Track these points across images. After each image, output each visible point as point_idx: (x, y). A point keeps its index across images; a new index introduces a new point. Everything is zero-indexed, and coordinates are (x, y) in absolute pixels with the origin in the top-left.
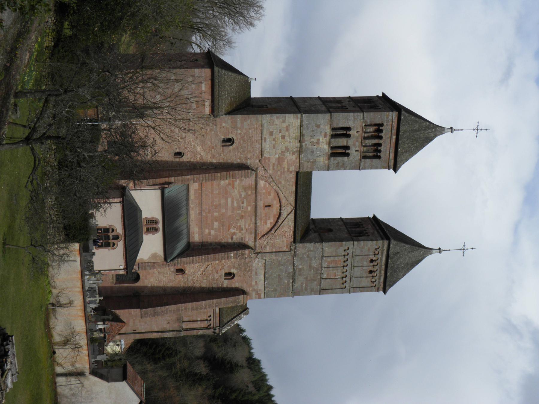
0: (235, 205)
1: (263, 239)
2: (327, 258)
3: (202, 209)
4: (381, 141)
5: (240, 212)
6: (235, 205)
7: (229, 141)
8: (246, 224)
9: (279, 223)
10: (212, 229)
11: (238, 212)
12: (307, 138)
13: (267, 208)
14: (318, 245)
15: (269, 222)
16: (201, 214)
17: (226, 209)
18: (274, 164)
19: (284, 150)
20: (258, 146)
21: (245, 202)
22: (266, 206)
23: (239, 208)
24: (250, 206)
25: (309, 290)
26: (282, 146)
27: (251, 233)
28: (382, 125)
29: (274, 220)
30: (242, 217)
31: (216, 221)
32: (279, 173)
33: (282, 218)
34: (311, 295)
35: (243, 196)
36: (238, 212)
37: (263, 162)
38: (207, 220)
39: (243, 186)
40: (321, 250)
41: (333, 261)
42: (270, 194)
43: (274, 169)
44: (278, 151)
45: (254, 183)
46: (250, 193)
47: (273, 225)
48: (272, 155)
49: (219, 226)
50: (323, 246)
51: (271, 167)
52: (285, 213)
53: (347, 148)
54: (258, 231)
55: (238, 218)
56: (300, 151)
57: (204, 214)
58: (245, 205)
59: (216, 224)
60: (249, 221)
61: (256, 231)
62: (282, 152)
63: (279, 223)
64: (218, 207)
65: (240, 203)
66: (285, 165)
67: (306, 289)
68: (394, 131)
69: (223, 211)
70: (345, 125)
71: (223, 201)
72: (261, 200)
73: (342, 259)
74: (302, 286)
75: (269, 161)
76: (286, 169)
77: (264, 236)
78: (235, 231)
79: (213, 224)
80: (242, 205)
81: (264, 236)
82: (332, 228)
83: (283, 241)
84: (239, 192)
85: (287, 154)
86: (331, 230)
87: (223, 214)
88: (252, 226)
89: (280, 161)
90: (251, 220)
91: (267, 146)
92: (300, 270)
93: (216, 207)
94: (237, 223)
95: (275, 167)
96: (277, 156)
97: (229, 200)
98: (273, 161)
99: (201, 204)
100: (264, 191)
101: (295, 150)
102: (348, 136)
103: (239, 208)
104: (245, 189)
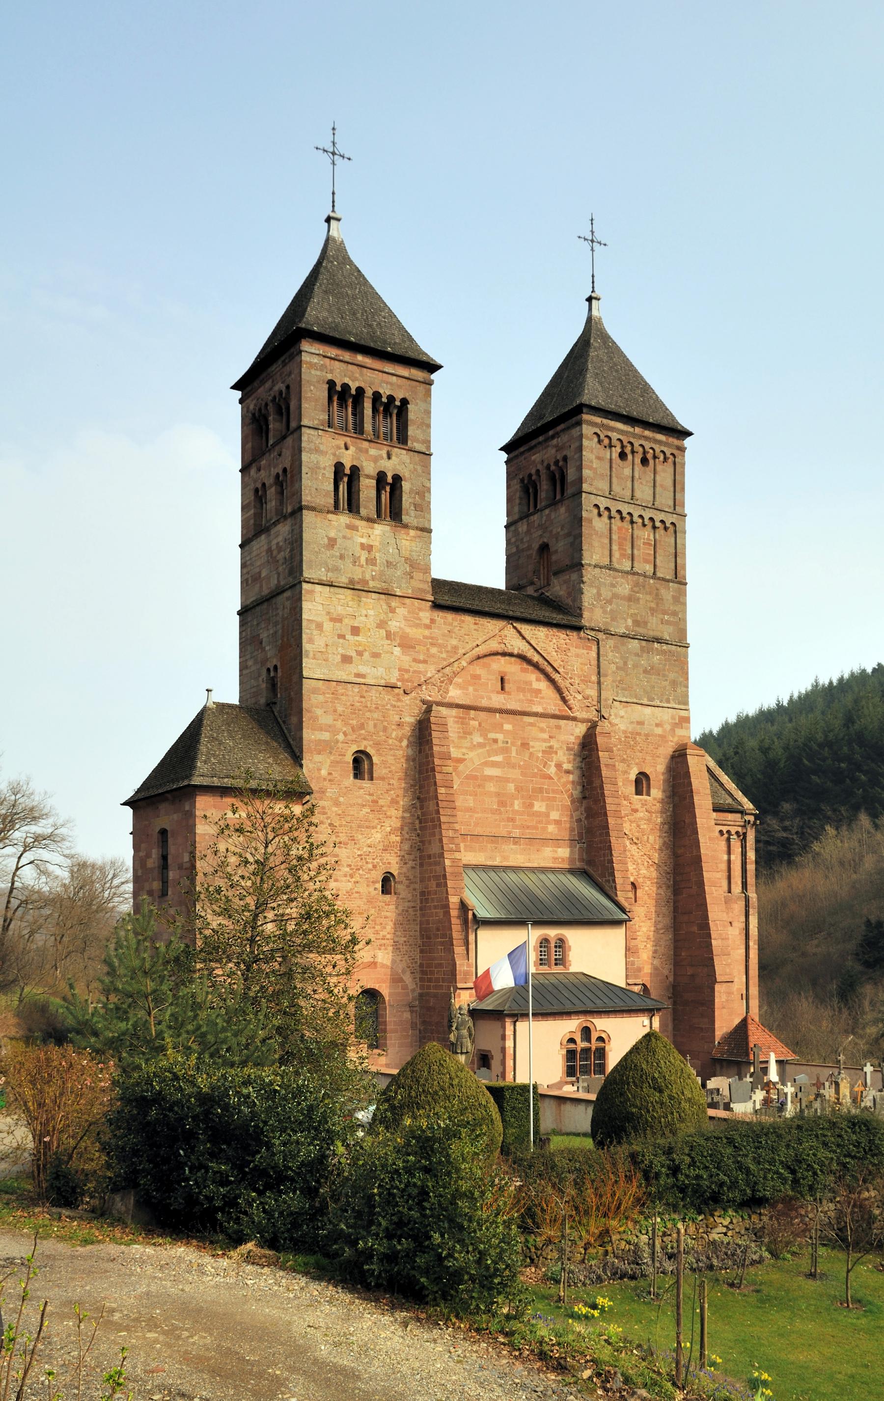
0: (499, 758)
2: (614, 559)
3: (507, 838)
5: (514, 748)
6: (499, 758)
9: (541, 661)
10: (547, 815)
11: (514, 754)
13: (507, 686)
14: (588, 574)
15: (536, 685)
16: (516, 840)
17: (507, 780)
18: (415, 660)
19: (383, 633)
20: (373, 693)
21: (492, 735)
22: (503, 689)
24: (502, 726)
26: (374, 638)
27: (558, 727)
29: (532, 672)
30: (525, 745)
31: (531, 805)
32: (434, 650)
33: (530, 654)
36: (514, 754)
38: (528, 827)
39: (460, 737)
40: (597, 570)
41: (620, 544)
42: (476, 677)
47: (542, 676)
48: (391, 664)
49: (543, 800)
50: (590, 565)
51: (421, 667)
52: (517, 645)
55: (527, 755)
57: (516, 833)
58: (500, 737)
59: (539, 806)
60: (534, 732)
61: (554, 717)
63: (541, 661)
65: (495, 746)
66: (416, 633)
69: (511, 787)
71: (491, 787)
72: (490, 699)
73: (617, 523)
75: (407, 671)
76: (427, 632)
77: (564, 700)
78: (553, 764)
79: (538, 814)
80: (500, 744)
81: (564, 700)
82: (536, 546)
83: (577, 656)
84: (473, 747)
85: (394, 625)
86: (544, 548)
87: (517, 789)
88: (543, 723)
89: (407, 644)
90: (531, 724)
93: (502, 804)
94: (538, 758)
95: (421, 658)
96: (397, 651)
99: (494, 838)
100: (471, 689)
101: (385, 607)
103: (505, 750)
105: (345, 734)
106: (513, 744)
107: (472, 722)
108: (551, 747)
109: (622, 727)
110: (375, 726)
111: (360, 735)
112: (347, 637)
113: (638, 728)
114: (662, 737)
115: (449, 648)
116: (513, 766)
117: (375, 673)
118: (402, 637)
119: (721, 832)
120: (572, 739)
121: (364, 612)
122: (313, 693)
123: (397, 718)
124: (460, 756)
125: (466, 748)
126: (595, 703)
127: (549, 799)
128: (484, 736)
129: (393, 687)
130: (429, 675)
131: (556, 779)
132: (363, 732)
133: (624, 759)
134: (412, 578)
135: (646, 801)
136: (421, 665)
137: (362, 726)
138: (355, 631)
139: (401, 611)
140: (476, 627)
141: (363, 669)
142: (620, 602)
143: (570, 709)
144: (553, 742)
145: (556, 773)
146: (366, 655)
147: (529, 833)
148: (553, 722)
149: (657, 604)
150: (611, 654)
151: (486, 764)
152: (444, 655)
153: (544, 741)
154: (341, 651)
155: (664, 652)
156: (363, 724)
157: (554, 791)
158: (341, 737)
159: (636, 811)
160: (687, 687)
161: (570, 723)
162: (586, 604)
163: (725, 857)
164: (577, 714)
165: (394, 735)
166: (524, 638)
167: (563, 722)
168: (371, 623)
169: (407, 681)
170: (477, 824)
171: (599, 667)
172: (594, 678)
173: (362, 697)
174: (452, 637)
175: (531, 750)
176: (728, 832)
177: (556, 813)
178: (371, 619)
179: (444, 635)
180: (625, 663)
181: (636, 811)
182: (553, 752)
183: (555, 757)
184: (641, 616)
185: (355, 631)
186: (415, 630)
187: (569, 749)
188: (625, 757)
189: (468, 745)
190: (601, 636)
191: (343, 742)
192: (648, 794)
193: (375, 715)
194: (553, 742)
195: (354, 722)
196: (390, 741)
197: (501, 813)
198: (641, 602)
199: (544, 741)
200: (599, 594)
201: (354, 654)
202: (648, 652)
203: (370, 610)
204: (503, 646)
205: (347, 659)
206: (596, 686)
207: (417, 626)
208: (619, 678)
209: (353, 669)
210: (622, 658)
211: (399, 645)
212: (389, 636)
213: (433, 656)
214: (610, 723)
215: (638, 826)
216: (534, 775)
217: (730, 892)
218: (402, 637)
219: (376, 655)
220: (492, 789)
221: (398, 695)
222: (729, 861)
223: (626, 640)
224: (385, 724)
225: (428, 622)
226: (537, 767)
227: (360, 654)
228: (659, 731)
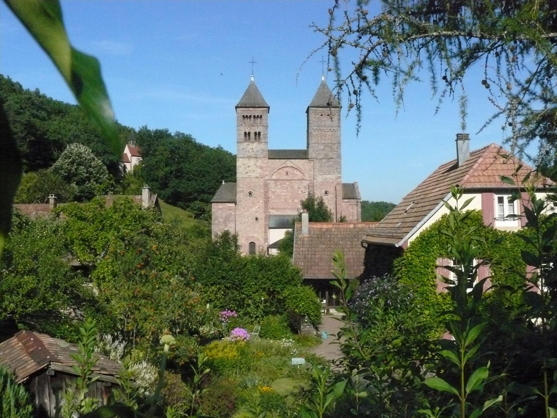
4: (252, 116)
8: (296, 185)
12: (249, 155)
15: (296, 173)
16: (289, 209)
23: (287, 189)
30: (292, 187)
53: (256, 133)
54: (301, 178)
56: (256, 158)
57: (290, 207)
64: (286, 200)
68: (247, 109)
69: (288, 197)
70: (243, 135)
84: (278, 189)
85: (258, 164)
88: (297, 182)
91: (253, 175)
96: (259, 170)
97: (282, 194)
99: (284, 209)
102: (249, 133)
103: (287, 189)
104: (276, 186)
138: (249, 167)
139: (260, 161)
185: (249, 167)
203: (252, 162)
205: (247, 173)
212: (257, 167)
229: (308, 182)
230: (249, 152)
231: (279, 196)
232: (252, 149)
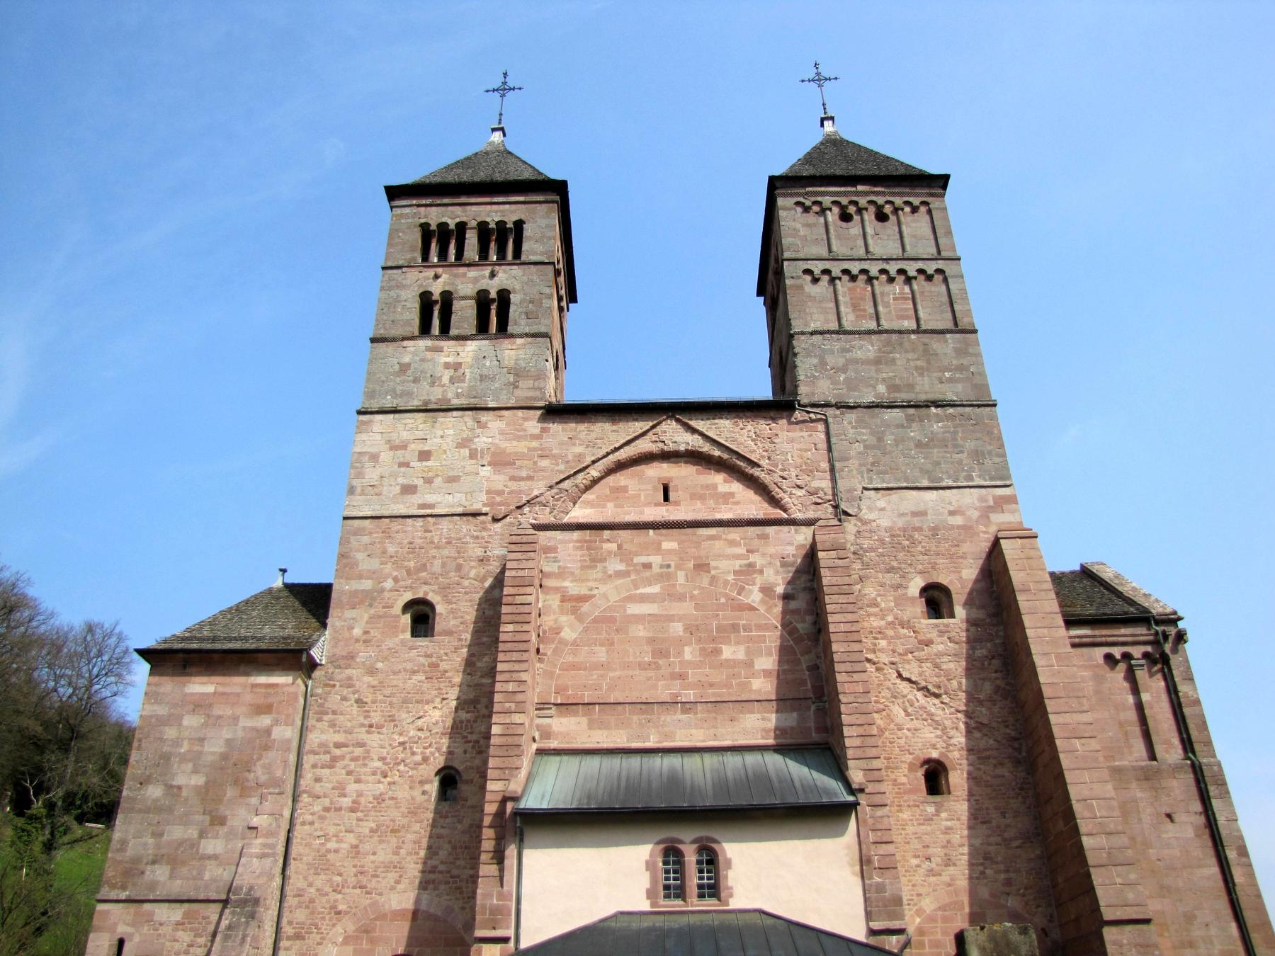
0: (655, 589)
1: (786, 499)
6: (655, 589)
7: (422, 617)
10: (749, 664)
16: (688, 707)
17: (670, 618)
18: (513, 478)
19: (466, 452)
21: (643, 559)
24: (660, 544)
25: (965, 362)
27: (764, 537)
28: (425, 228)
30: (702, 567)
32: (545, 463)
33: (706, 448)
34: (979, 355)
35: (621, 567)
37: (503, 510)
38: (711, 685)
39: (583, 568)
43: (530, 478)
44: (468, 469)
45: (576, 535)
46: (614, 546)
49: (738, 643)
51: (524, 485)
57: (690, 695)
58: (656, 560)
59: (728, 652)
60: (718, 545)
62: (473, 455)
65: (647, 574)
66: (512, 446)
67: (961, 368)
69: (678, 629)
70: (415, 306)
74: (950, 380)
75: (500, 493)
76: (535, 444)
78: (756, 588)
80: (656, 569)
83: (792, 441)
85: (482, 442)
88: (735, 534)
90: (712, 538)
92: (893, 388)
93: (661, 653)
94: (726, 582)
95: (524, 474)
97: (634, 609)
98: (500, 481)
101: (470, 423)
103: (666, 576)
104: (596, 560)
105: (396, 580)
106: (678, 567)
107: (606, 546)
108: (751, 565)
109: (885, 523)
110: (444, 565)
111: (419, 579)
112: (412, 464)
113: (916, 521)
114: (966, 528)
115: (570, 457)
116: (681, 598)
117: (446, 501)
118: (494, 454)
119: (1109, 658)
120: (791, 550)
121: (440, 433)
122: (355, 534)
123: (479, 552)
124: (584, 591)
125: (595, 580)
126: (830, 497)
127: (750, 639)
128: (629, 562)
129: (475, 515)
130: (536, 493)
131: (762, 610)
132: (424, 574)
133: (893, 568)
134: (517, 387)
135: (947, 626)
136: (522, 483)
137: (423, 567)
140: (615, 427)
141: (430, 498)
142: (860, 367)
143: (785, 510)
144: (753, 558)
145: (762, 601)
146: (438, 481)
147: (711, 694)
148: (751, 530)
149: (928, 362)
150: (851, 431)
151: (631, 599)
152: (562, 467)
153: (738, 557)
154: (401, 480)
155: (953, 416)
156: (425, 565)
157: (759, 627)
158: (389, 584)
159: (928, 643)
160: (1004, 456)
161: (785, 529)
162: (802, 378)
163: (1130, 699)
164: (799, 516)
165: (473, 573)
166: (694, 431)
167: (771, 530)
168: (449, 443)
169: (499, 504)
170: (611, 688)
171: (830, 449)
172: (825, 465)
173: (426, 531)
174: (574, 445)
175: (713, 572)
176: (1127, 657)
177: (758, 663)
178: (449, 440)
179: (562, 443)
180: (880, 439)
181: (928, 643)
182: (755, 572)
183: (759, 580)
184: (901, 378)
186: (515, 443)
187: (783, 565)
188: (895, 564)
189: (600, 575)
190: (830, 412)
191: (391, 590)
192: (952, 616)
193: (446, 552)
194: (753, 558)
195: (412, 564)
196: (466, 583)
197: (658, 667)
198: (899, 362)
199: (738, 557)
200: (823, 363)
201: (419, 482)
202: (922, 421)
203: (451, 426)
204: (661, 445)
206: (828, 475)
207: (519, 438)
208: (871, 460)
209: (416, 499)
210: (872, 433)
211: (489, 464)
212: (473, 455)
213: (543, 469)
214: (861, 520)
215: (937, 666)
216: (723, 607)
217: (1152, 756)
218: (494, 454)
219: (453, 480)
220: (641, 634)
221: (483, 522)
222: (1140, 707)
223: (877, 410)
224: (461, 561)
225: (537, 431)
226: (726, 595)
227: (429, 481)
228: (958, 520)
229: (803, 536)
230: (434, 381)
231: (610, 625)
232: (457, 366)
